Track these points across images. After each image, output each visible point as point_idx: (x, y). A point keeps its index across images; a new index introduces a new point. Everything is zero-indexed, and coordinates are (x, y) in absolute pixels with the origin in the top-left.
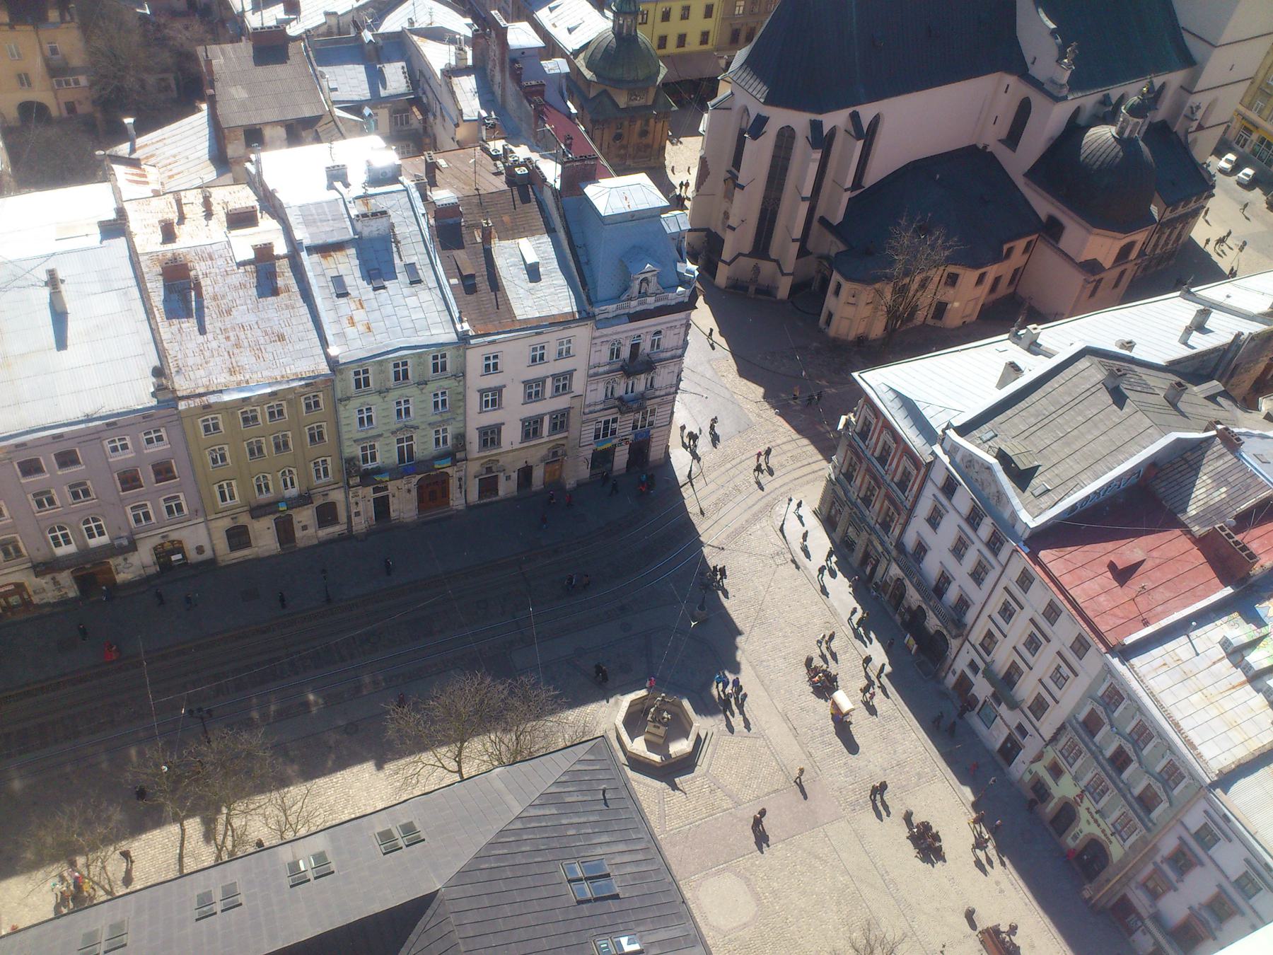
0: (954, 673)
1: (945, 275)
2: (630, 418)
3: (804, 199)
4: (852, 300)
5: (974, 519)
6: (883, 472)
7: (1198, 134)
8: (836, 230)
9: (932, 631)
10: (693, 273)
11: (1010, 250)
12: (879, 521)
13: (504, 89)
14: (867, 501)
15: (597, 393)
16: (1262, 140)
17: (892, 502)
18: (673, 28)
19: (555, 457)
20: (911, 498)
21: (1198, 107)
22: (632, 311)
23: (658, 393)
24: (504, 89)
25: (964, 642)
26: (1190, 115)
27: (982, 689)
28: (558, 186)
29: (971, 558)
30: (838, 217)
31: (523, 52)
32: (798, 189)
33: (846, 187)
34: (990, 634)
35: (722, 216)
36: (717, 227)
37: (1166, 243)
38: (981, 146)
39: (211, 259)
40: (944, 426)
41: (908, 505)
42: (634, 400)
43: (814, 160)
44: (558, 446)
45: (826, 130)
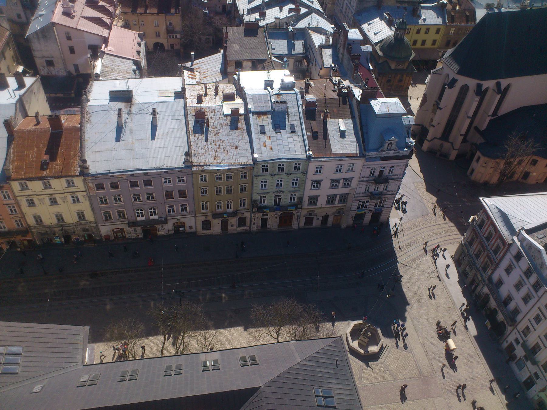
0: (507, 342)
1: (531, 160)
2: (375, 201)
3: (468, 117)
4: (484, 165)
5: (528, 273)
6: (487, 245)
8: (482, 133)
9: (499, 321)
10: (413, 143)
12: (482, 266)
13: (343, 56)
14: (477, 256)
15: (362, 189)
17: (490, 259)
18: (421, 37)
19: (339, 213)
20: (499, 258)
22: (382, 156)
23: (388, 193)
24: (343, 56)
25: (514, 329)
27: (520, 352)
28: (359, 99)
29: (524, 291)
30: (484, 127)
31: (354, 41)
32: (467, 113)
34: (527, 328)
36: (426, 125)
39: (214, 112)
40: (520, 228)
41: (497, 261)
42: (378, 194)
44: (341, 209)
45: (484, 88)
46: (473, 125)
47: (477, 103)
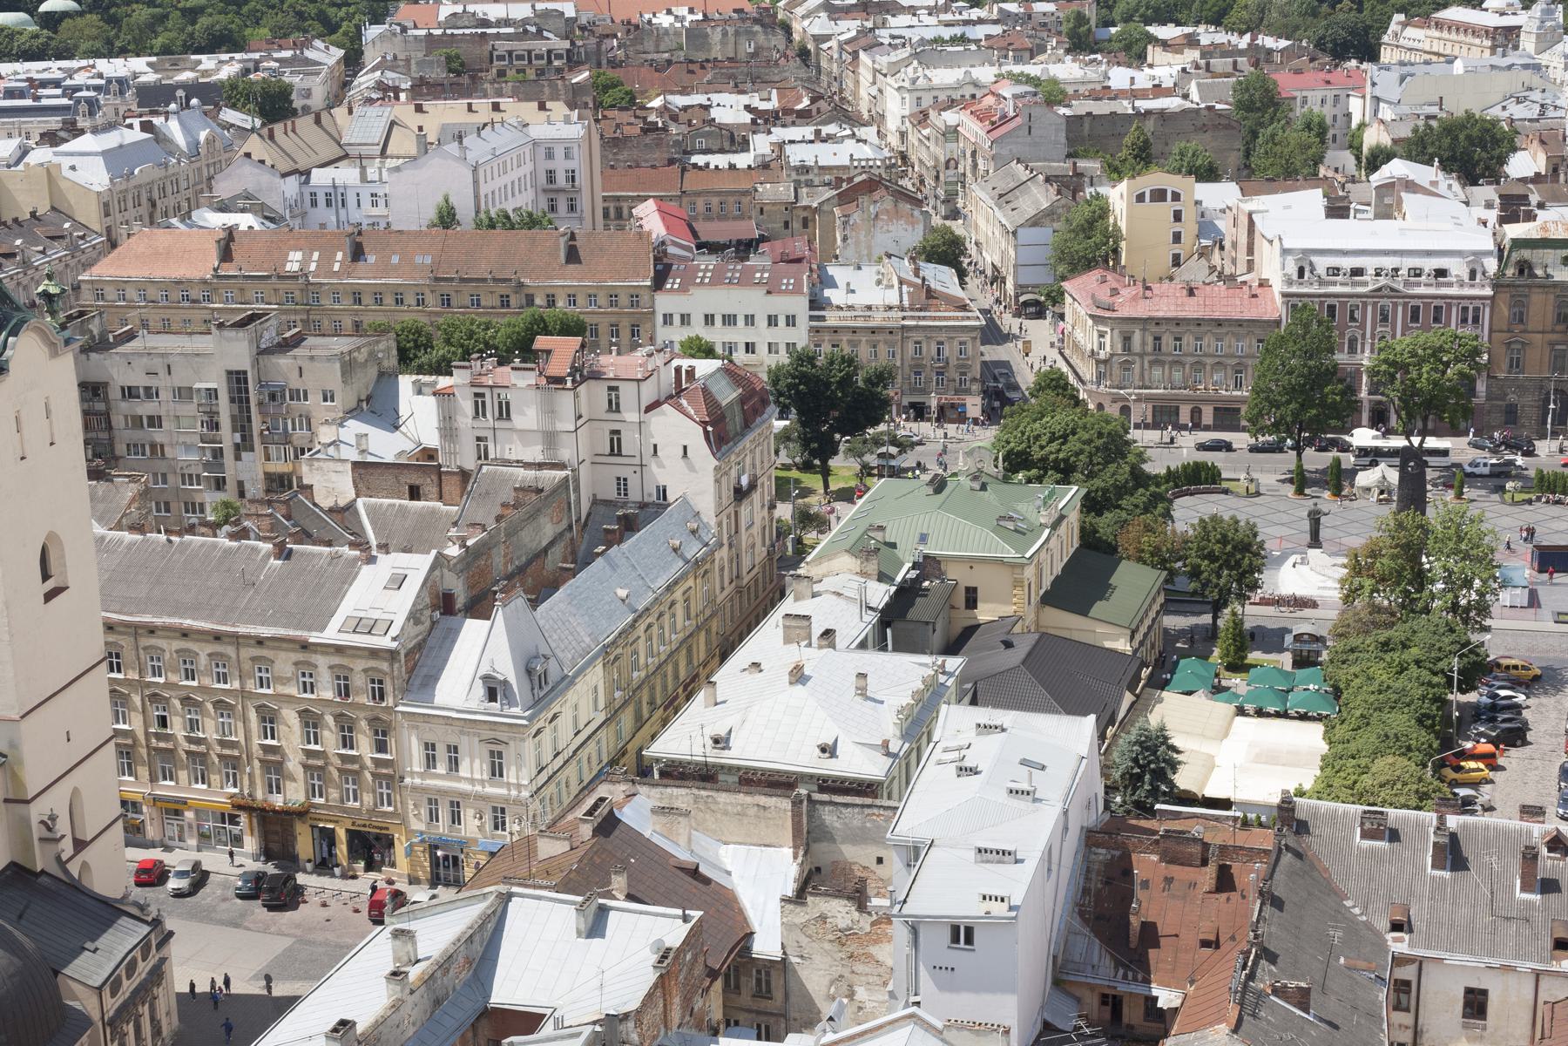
7: (87, 855)
21: (53, 818)
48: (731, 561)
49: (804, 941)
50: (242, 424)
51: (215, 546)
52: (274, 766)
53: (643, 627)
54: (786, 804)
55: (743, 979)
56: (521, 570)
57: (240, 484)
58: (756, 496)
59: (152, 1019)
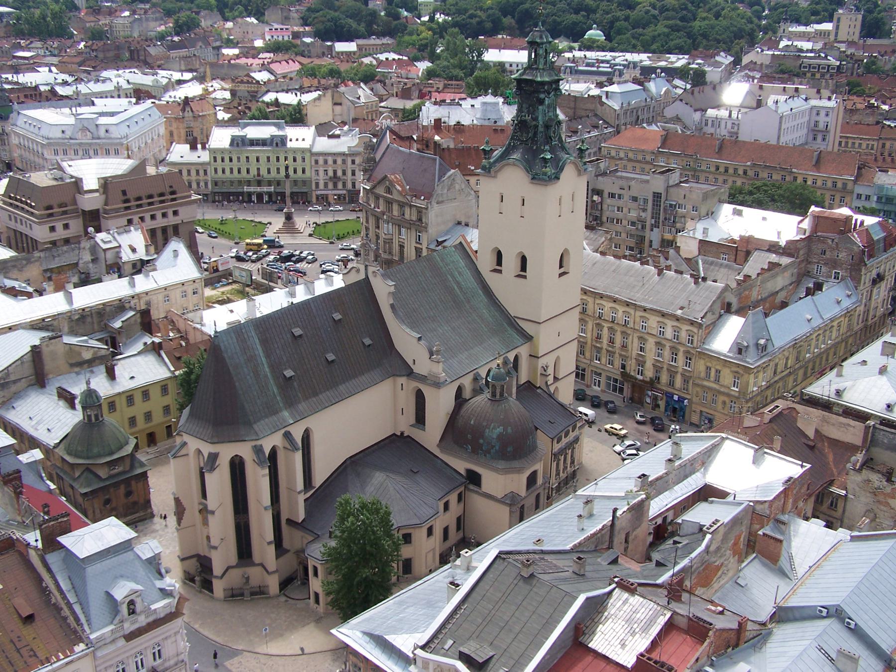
3: (266, 508)
7: (558, 384)
10: (174, 586)
11: (446, 507)
16: (609, 378)
18: (139, 408)
22: (127, 632)
26: (544, 373)
28: (40, 545)
30: (301, 516)
33: (298, 490)
35: (205, 539)
37: (565, 468)
38: (399, 434)
40: (412, 649)
43: (264, 476)
46: (283, 522)
47: (268, 478)
48: (864, 312)
49: (857, 489)
50: (655, 215)
51: (633, 266)
52: (641, 363)
53: (816, 334)
54: (859, 426)
55: (825, 499)
56: (763, 300)
57: (651, 241)
58: (883, 284)
59: (572, 456)
